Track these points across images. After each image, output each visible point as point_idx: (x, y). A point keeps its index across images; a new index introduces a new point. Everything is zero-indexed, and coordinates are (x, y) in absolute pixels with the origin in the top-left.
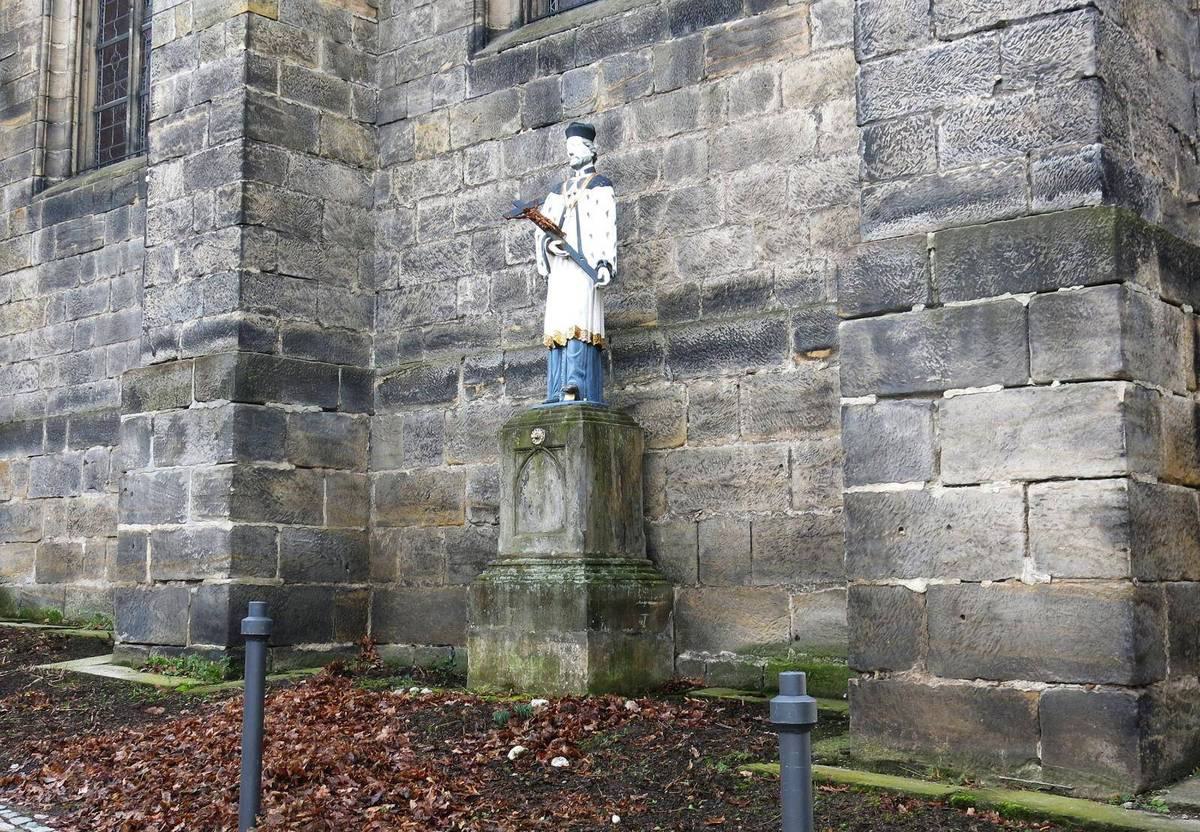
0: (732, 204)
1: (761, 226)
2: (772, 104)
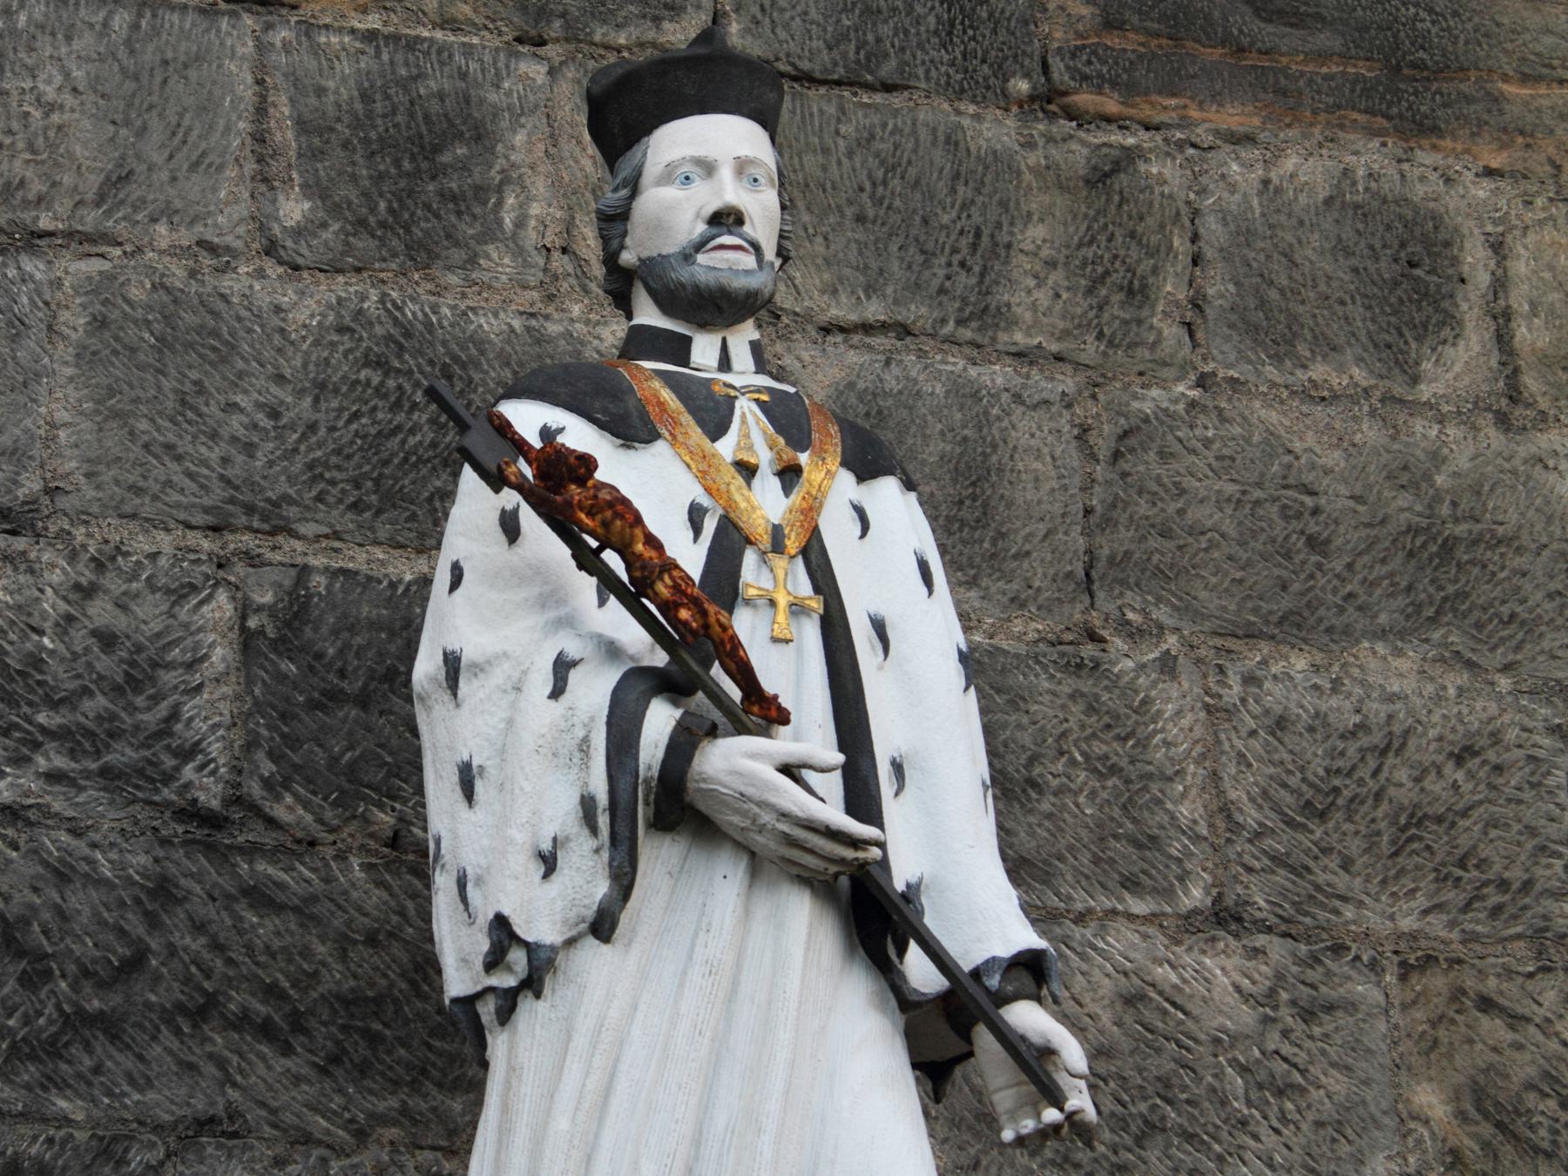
0: (1251, 816)
1: (1438, 982)
2: (1458, 365)
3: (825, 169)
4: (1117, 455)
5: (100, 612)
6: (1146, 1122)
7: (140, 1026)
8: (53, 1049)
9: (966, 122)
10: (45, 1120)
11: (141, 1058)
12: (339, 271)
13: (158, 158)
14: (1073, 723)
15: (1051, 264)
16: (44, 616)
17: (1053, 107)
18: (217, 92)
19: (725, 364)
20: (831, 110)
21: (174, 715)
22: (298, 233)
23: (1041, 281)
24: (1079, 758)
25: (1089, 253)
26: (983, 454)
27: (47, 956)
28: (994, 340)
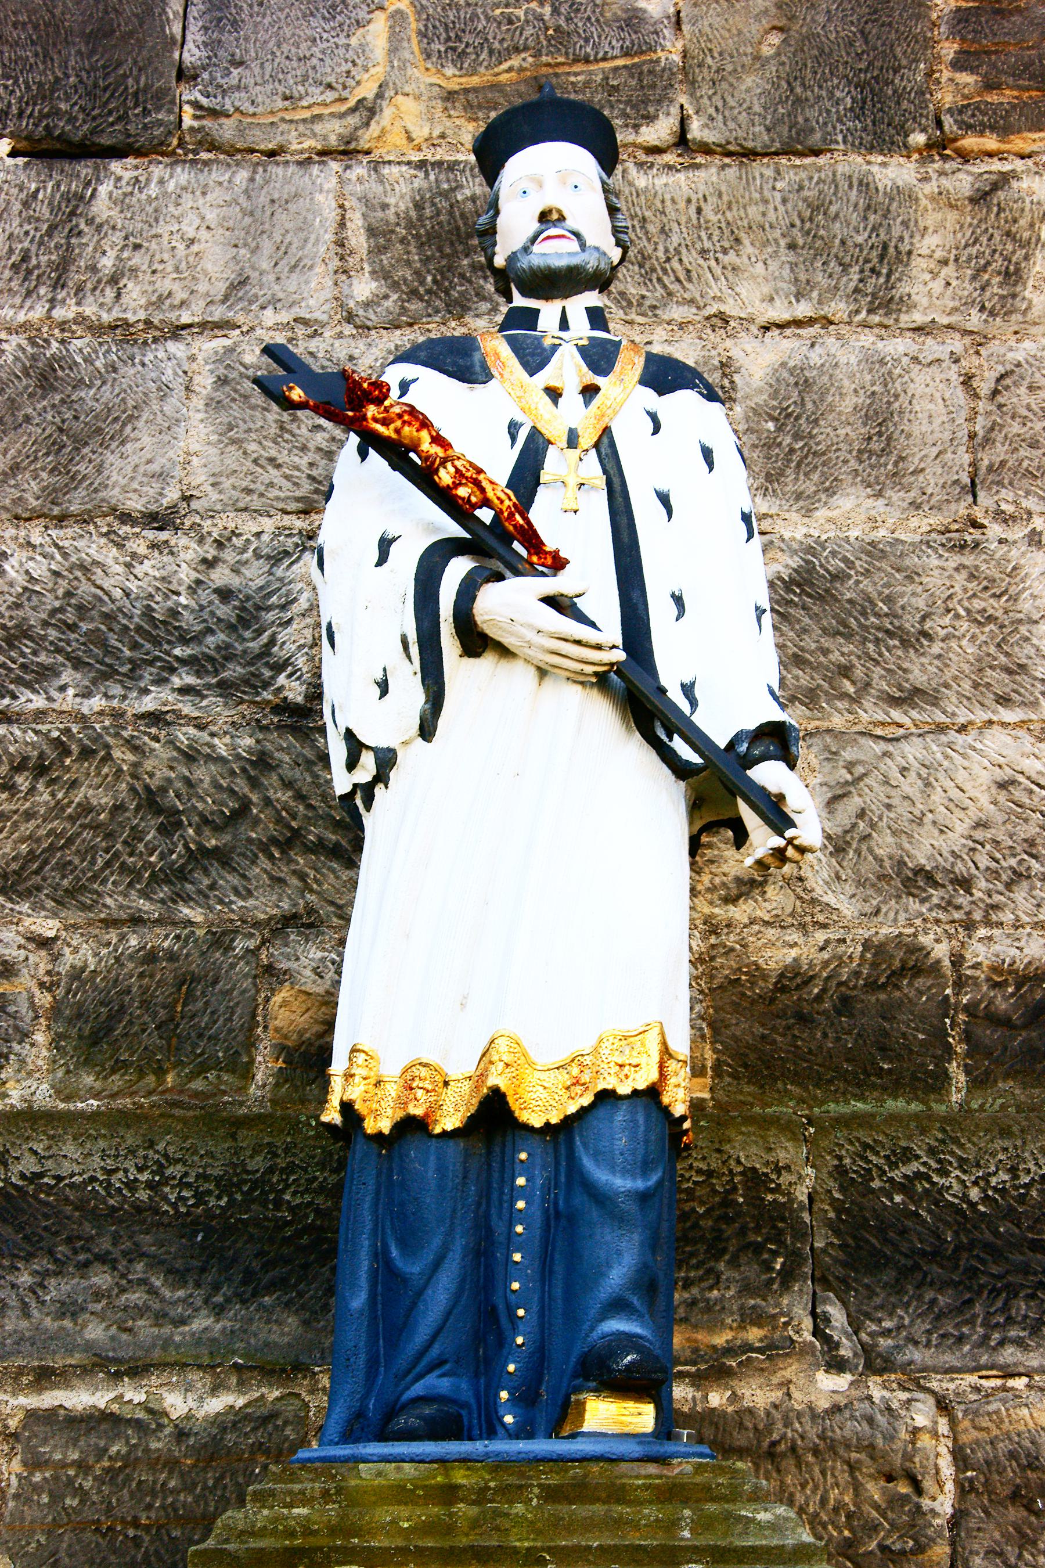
3: (764, 214)
4: (995, 393)
5: (220, 576)
6: (1015, 872)
7: (244, 855)
8: (182, 875)
9: (875, 169)
10: (174, 924)
11: (244, 876)
12: (398, 327)
13: (265, 265)
14: (958, 588)
15: (945, 262)
16: (180, 583)
17: (947, 152)
18: (310, 217)
19: (564, 325)
20: (769, 172)
21: (272, 641)
22: (367, 305)
23: (935, 275)
24: (963, 613)
25: (973, 250)
26: (889, 403)
27: (178, 812)
28: (897, 320)
